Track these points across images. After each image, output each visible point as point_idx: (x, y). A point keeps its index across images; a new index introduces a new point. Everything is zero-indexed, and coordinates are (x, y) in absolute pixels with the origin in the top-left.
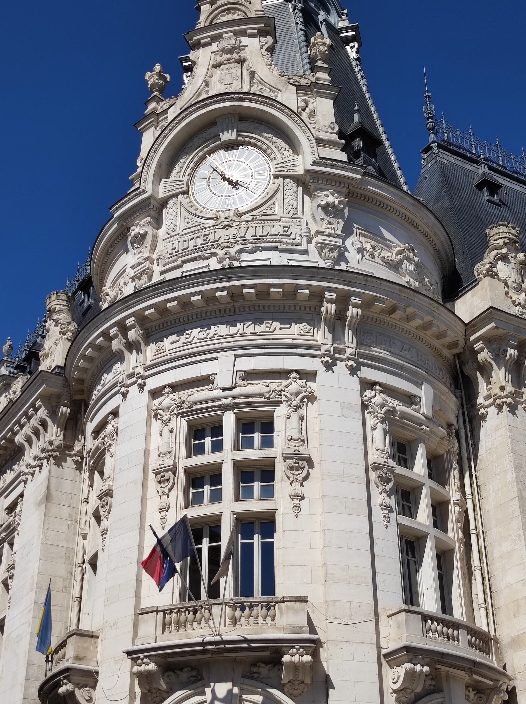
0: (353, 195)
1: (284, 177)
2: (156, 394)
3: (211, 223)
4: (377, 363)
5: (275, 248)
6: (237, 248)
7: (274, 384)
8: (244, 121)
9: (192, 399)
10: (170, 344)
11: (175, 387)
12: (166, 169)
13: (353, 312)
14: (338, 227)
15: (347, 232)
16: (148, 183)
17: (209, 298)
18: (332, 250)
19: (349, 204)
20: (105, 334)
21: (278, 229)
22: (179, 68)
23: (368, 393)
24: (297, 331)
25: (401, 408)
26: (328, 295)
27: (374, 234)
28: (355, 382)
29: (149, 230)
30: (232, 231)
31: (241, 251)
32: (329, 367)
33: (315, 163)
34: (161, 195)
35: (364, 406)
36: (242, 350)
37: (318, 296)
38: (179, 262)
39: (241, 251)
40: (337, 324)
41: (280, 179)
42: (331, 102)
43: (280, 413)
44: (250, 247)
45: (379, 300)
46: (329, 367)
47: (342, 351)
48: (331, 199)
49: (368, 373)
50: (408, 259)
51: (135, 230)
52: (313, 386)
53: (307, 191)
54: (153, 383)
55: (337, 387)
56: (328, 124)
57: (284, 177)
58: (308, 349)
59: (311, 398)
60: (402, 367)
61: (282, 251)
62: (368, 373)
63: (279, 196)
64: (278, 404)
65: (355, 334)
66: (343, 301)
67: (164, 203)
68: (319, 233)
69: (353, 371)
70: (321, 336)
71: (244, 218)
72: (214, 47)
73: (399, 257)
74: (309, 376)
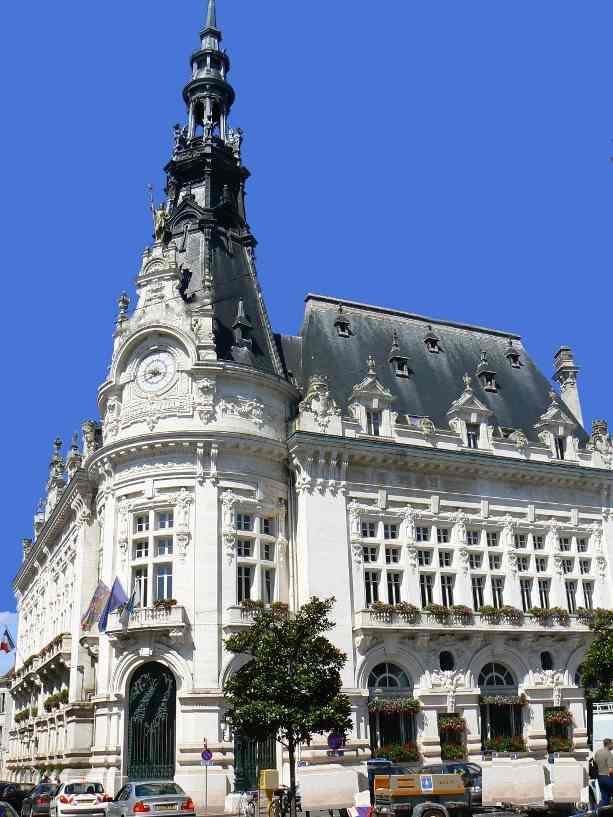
0: (220, 377)
2: (119, 499)
4: (229, 478)
5: (175, 416)
8: (159, 340)
10: (125, 475)
11: (127, 496)
12: (123, 367)
13: (214, 451)
14: (211, 398)
15: (216, 402)
16: (112, 377)
17: (139, 449)
22: (129, 307)
24: (186, 467)
25: (242, 499)
26: (199, 445)
27: (230, 399)
29: (116, 402)
30: (154, 406)
31: (158, 418)
32: (201, 483)
34: (121, 381)
35: (220, 502)
36: (156, 477)
37: (193, 444)
39: (158, 418)
40: (206, 458)
44: (163, 416)
46: (201, 483)
47: (208, 474)
48: (206, 384)
49: (223, 484)
50: (256, 408)
51: (109, 403)
52: (193, 495)
53: (194, 379)
54: (119, 493)
55: (207, 494)
57: (182, 371)
58: (191, 475)
59: (191, 501)
61: (180, 417)
62: (223, 484)
64: (174, 505)
65: (216, 464)
66: (207, 446)
67: (122, 387)
68: (200, 404)
69: (215, 484)
70: (198, 468)
72: (149, 287)
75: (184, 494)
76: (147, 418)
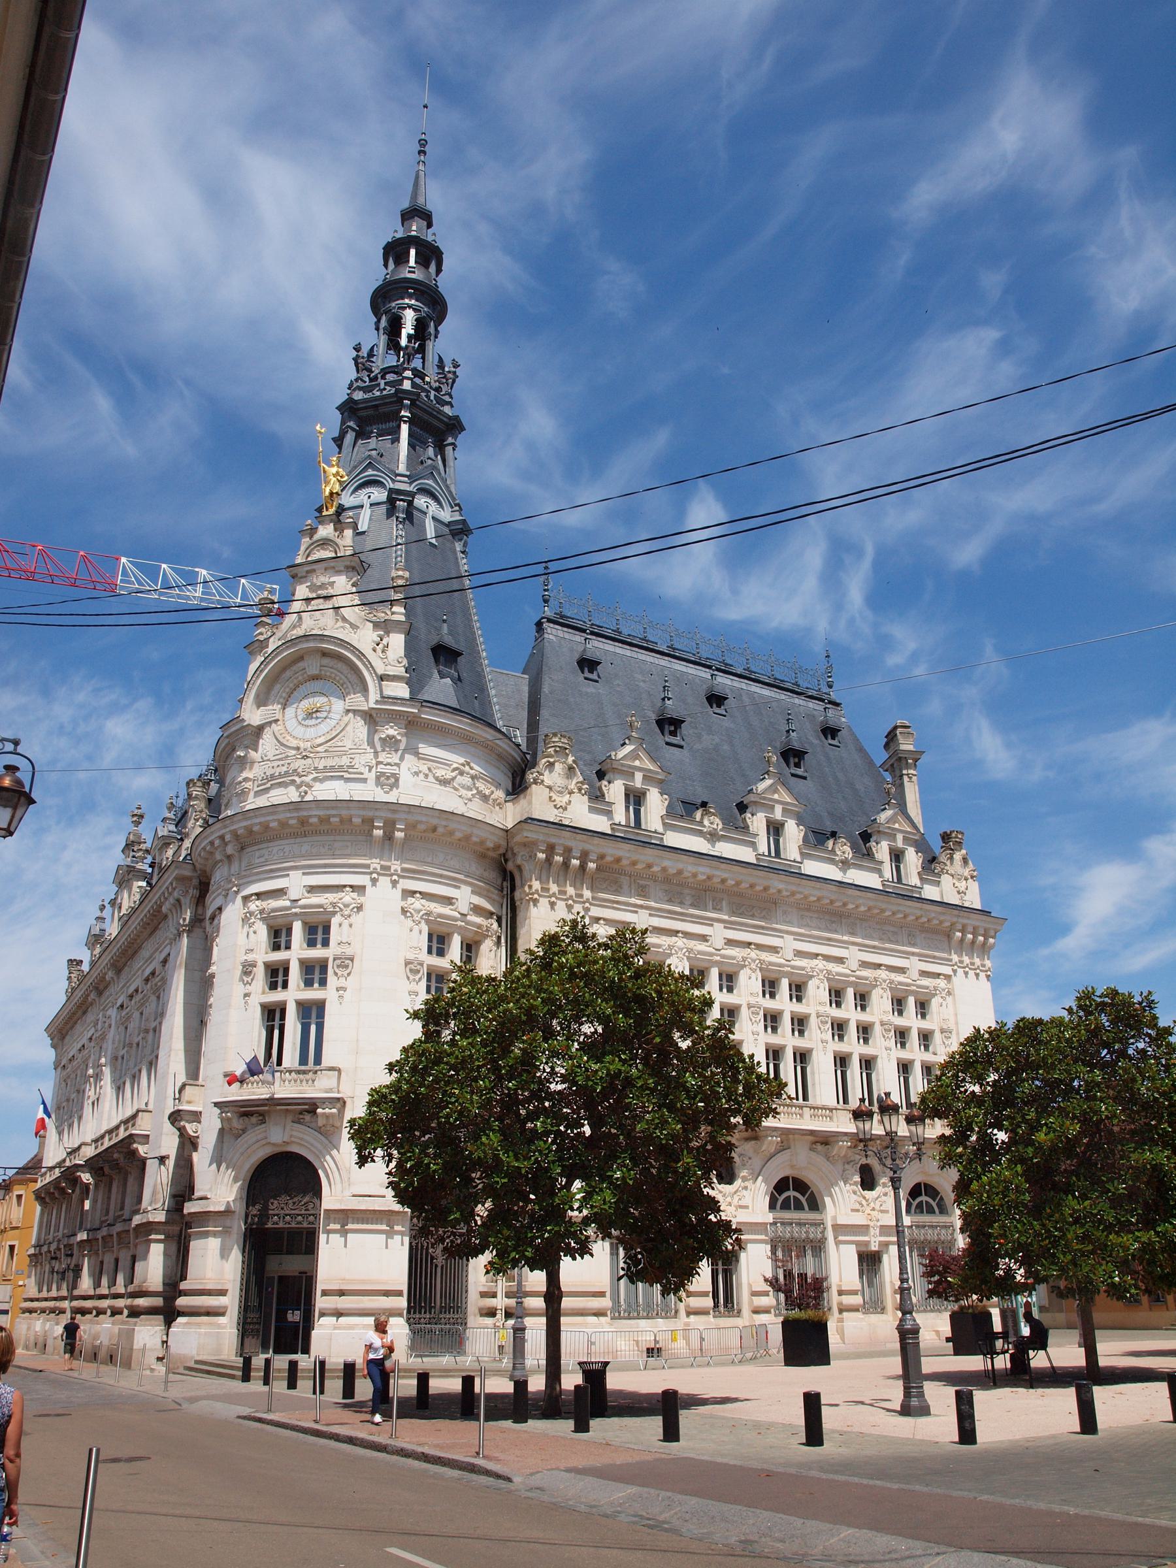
1: (355, 712)
3: (294, 752)
6: (311, 777)
7: (331, 897)
9: (270, 906)
18: (388, 778)
19: (406, 735)
20: (212, 843)
21: (345, 761)
23: (410, 900)
25: (438, 908)
28: (398, 893)
33: (377, 702)
38: (268, 785)
41: (351, 715)
42: (403, 636)
43: (335, 921)
45: (421, 822)
48: (391, 732)
56: (397, 657)
60: (441, 876)
63: (348, 728)
71: (318, 749)
73: (454, 774)
74: (359, 889)
75: (348, 897)
76: (296, 778)
